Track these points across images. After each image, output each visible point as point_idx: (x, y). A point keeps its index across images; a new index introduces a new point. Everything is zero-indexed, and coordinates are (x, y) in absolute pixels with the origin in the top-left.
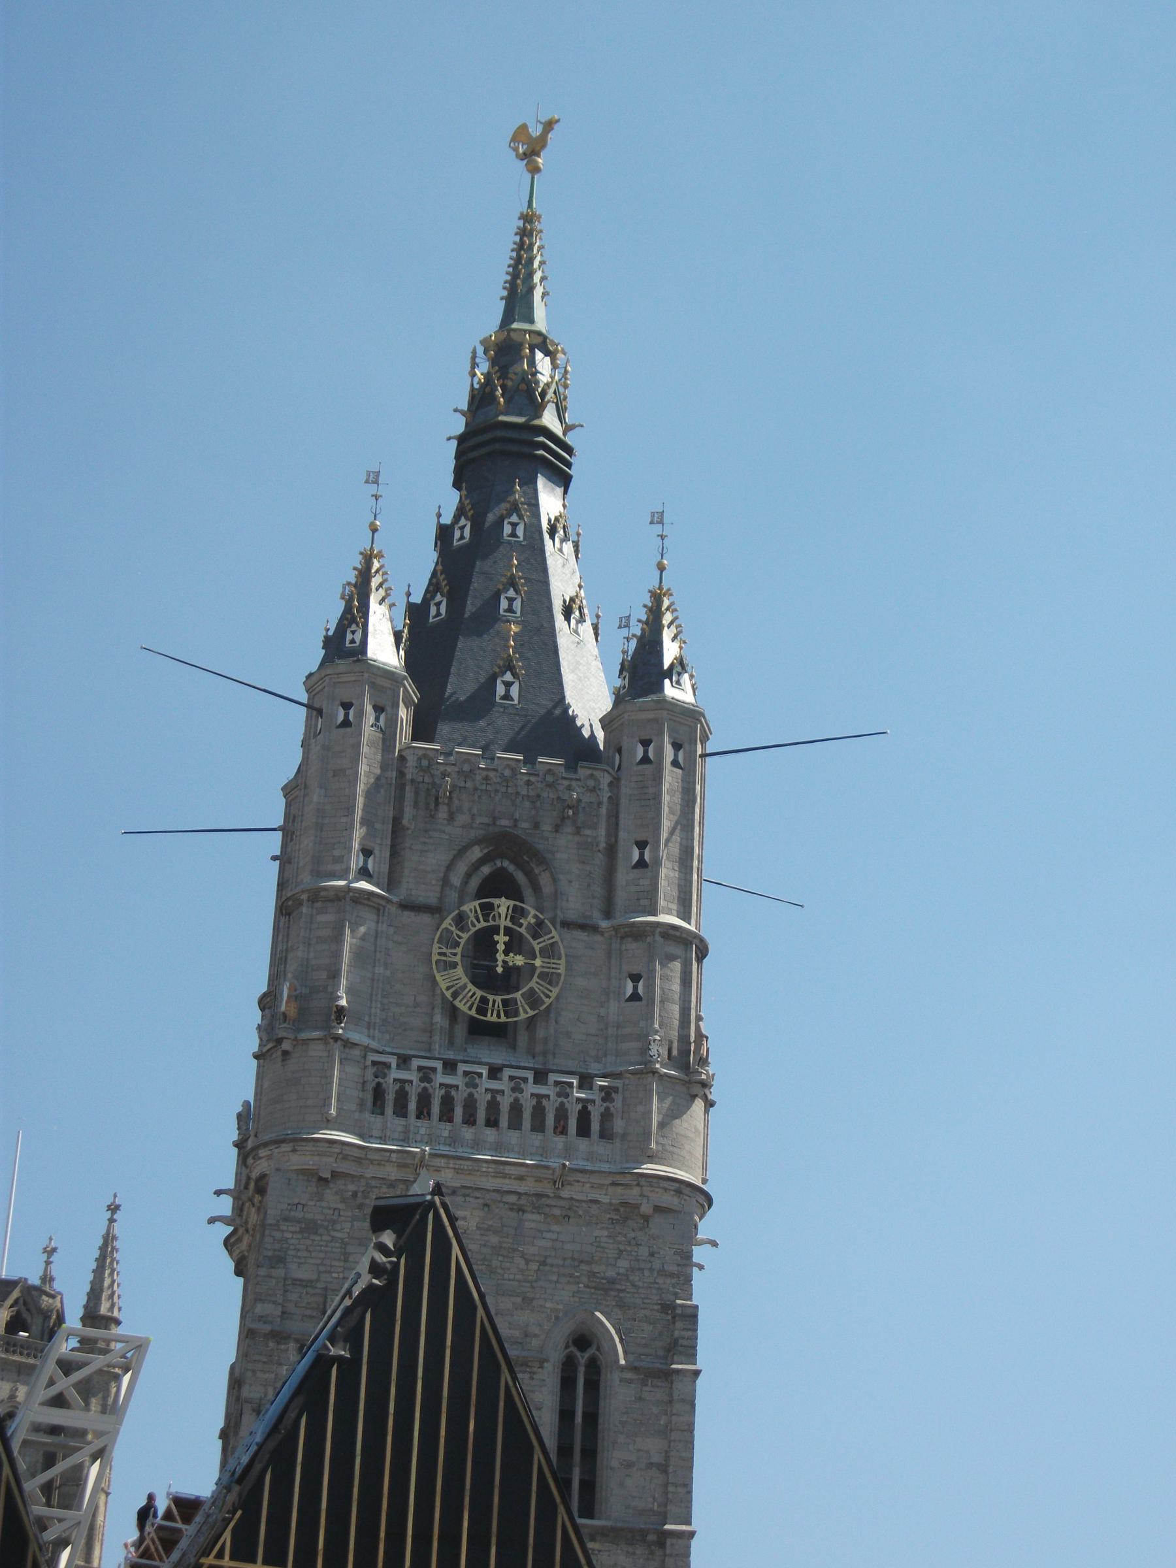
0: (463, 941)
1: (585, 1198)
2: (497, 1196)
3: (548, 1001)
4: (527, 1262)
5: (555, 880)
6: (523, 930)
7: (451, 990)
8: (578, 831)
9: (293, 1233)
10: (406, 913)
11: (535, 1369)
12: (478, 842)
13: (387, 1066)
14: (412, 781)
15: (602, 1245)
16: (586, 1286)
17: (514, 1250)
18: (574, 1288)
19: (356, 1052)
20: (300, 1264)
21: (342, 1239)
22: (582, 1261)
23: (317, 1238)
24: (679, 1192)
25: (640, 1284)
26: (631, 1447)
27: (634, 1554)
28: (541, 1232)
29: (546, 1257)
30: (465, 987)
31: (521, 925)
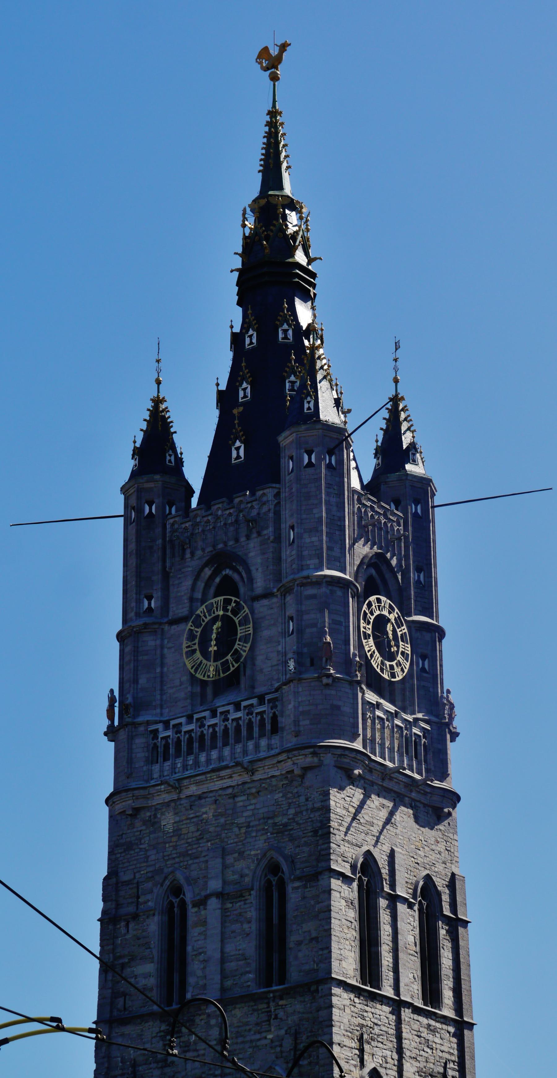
0: (198, 634)
1: (266, 777)
2: (220, 792)
3: (244, 654)
4: (240, 828)
5: (248, 571)
6: (229, 614)
7: (194, 668)
8: (259, 534)
9: (121, 853)
10: (173, 627)
11: (247, 897)
12: (206, 565)
14: (171, 541)
15: (279, 803)
16: (272, 834)
17: (233, 823)
18: (265, 837)
19: (142, 729)
20: (124, 871)
21: (145, 848)
22: (268, 818)
23: (132, 852)
24: (314, 754)
25: (301, 822)
26: (300, 932)
27: (304, 1001)
28: (246, 806)
29: (249, 822)
30: (201, 662)
31: (227, 611)
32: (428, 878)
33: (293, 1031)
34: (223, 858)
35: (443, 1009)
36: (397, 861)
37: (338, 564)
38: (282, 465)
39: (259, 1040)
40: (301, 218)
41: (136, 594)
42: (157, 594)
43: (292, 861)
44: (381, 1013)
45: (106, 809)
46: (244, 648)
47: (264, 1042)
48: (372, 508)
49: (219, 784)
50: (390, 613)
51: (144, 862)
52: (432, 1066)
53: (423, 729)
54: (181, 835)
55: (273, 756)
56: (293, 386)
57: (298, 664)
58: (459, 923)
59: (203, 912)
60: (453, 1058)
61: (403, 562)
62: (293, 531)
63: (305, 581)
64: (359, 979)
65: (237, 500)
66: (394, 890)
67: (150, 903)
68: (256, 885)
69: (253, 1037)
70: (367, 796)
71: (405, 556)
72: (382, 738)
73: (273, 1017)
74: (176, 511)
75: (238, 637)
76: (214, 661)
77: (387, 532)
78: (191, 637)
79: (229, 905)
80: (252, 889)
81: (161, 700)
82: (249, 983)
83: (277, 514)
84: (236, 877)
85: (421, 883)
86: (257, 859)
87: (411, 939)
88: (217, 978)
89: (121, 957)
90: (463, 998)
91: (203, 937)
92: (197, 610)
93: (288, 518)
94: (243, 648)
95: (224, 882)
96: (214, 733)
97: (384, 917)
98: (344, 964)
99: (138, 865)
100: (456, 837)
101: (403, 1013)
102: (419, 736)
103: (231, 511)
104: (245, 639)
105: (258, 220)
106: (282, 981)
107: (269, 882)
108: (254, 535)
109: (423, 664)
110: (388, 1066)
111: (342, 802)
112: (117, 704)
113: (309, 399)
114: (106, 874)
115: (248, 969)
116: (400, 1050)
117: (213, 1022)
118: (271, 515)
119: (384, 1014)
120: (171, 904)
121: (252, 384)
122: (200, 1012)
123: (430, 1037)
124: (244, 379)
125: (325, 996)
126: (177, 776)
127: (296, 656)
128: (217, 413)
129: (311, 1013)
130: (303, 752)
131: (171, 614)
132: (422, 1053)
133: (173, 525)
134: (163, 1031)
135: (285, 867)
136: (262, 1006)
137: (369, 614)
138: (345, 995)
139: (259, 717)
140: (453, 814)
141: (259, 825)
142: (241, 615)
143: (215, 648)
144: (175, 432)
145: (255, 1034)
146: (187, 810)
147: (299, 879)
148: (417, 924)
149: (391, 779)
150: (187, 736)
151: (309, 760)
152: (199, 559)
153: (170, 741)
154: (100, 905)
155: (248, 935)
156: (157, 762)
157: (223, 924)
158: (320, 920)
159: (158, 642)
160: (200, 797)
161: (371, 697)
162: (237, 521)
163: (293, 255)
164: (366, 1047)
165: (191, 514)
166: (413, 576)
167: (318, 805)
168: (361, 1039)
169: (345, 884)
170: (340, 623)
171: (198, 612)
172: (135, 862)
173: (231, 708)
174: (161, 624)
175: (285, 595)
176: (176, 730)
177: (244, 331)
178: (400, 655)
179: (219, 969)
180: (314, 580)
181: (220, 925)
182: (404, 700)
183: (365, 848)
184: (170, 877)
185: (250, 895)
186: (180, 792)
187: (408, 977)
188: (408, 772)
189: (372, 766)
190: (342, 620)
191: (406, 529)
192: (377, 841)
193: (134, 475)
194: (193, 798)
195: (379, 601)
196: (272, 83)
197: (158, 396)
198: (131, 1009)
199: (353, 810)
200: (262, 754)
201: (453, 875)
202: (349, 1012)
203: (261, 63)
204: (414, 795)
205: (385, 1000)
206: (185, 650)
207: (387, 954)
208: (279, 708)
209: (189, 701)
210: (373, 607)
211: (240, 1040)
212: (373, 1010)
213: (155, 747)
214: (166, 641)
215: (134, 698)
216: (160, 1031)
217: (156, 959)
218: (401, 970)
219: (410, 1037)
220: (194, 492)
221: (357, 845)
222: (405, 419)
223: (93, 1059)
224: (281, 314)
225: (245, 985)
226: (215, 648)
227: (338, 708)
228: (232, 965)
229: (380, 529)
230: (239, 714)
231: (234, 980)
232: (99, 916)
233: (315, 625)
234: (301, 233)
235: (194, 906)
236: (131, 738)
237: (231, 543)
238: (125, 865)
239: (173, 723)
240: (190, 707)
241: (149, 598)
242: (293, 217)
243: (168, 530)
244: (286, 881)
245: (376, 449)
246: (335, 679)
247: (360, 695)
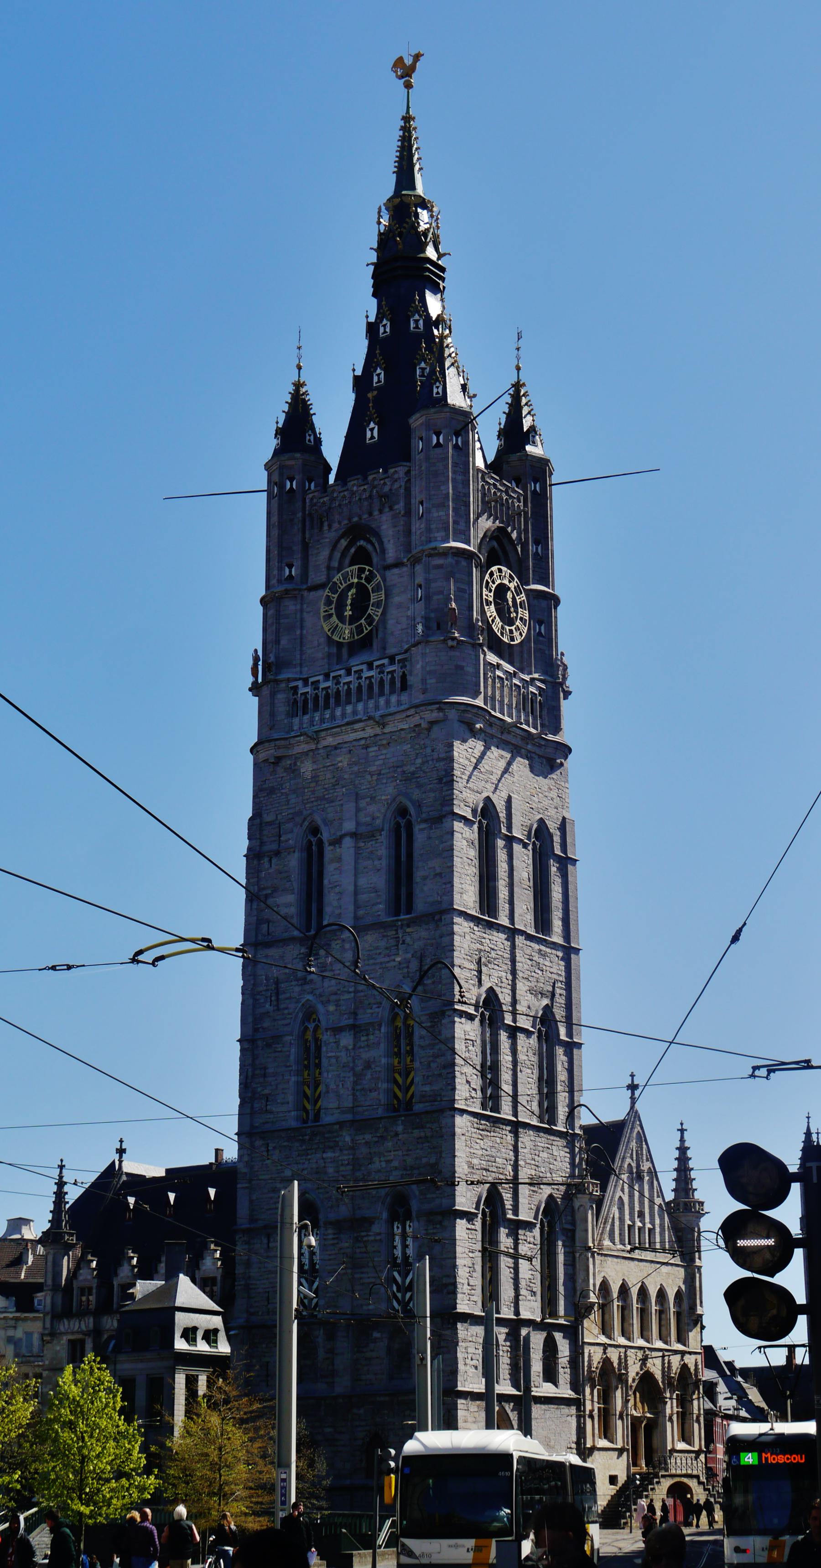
3: (377, 618)
4: (372, 775)
5: (381, 543)
6: (363, 581)
8: (391, 508)
9: (264, 797)
10: (312, 593)
13: (296, 688)
14: (310, 514)
18: (395, 784)
19: (283, 685)
22: (398, 767)
23: (274, 796)
24: (440, 709)
25: (427, 770)
27: (429, 929)
28: (377, 756)
29: (380, 770)
30: (337, 625)
31: (361, 578)
32: (541, 822)
33: (418, 954)
34: (356, 802)
35: (553, 936)
36: (513, 806)
37: (463, 537)
38: (413, 445)
39: (388, 962)
40: (432, 216)
41: (278, 562)
42: (297, 563)
43: (419, 805)
44: (498, 940)
45: (251, 757)
46: (376, 613)
47: (392, 964)
48: (495, 485)
49: (353, 736)
50: (510, 582)
51: (285, 805)
52: (542, 985)
53: (539, 688)
54: (318, 781)
55: (403, 711)
56: (423, 372)
57: (426, 627)
58: (569, 861)
59: (338, 850)
60: (561, 979)
61: (523, 535)
62: (422, 506)
63: (432, 552)
64: (478, 910)
65: (370, 478)
66: (511, 832)
67: (290, 841)
68: (386, 827)
69: (383, 960)
70: (487, 748)
71: (524, 530)
72: (502, 696)
73: (401, 942)
74: (315, 487)
75: (371, 602)
76: (350, 624)
77: (508, 508)
78: (329, 602)
79: (363, 844)
80: (383, 830)
81: (301, 659)
82: (379, 913)
83: (408, 490)
84: (368, 819)
85: (535, 826)
86: (387, 803)
87: (525, 875)
88: (351, 908)
89: (264, 889)
90: (571, 927)
91: (338, 872)
92: (334, 577)
93: (417, 493)
94: (375, 613)
95: (358, 824)
96: (349, 689)
97: (502, 856)
98: (465, 896)
99: (279, 808)
100: (567, 785)
101: (517, 940)
102: (536, 694)
103: (366, 487)
104: (378, 604)
105: (392, 218)
106: (409, 911)
107: (398, 825)
108: (387, 510)
109: (540, 629)
110: (503, 985)
111: (465, 753)
112: (260, 663)
113: (438, 384)
114: (251, 815)
115: (379, 901)
116: (514, 972)
117: (347, 946)
118: (402, 491)
119: (500, 940)
120: (310, 842)
121: (385, 370)
122: (335, 938)
123: (541, 961)
124: (378, 365)
125: (447, 924)
126: (316, 728)
127: (423, 621)
128: (353, 396)
129: (435, 939)
130: (430, 707)
131: (310, 581)
132: (533, 974)
133: (312, 499)
134: (303, 953)
135: (412, 811)
136: (391, 933)
137: (491, 583)
138: (466, 924)
139: (390, 676)
140: (565, 764)
141: (389, 772)
142: (374, 583)
143: (350, 613)
144: (314, 414)
145: (384, 957)
146: (324, 759)
147: (425, 821)
148: (530, 862)
149: (509, 732)
150: (324, 692)
151: (435, 715)
152: (335, 531)
153: (309, 697)
154: (246, 843)
155: (378, 870)
156: (297, 716)
157: (356, 862)
158: (444, 858)
159: (298, 607)
160: (336, 748)
161: (492, 658)
162: (370, 496)
163: (424, 251)
164: (484, 969)
165: (329, 490)
166: (531, 548)
167: (443, 755)
168: (479, 963)
169: (467, 826)
170: (463, 591)
171: (335, 580)
172: (277, 805)
173: (364, 667)
174: (300, 590)
175: (414, 565)
176: (314, 686)
177: (378, 321)
178: (518, 620)
179: (352, 900)
180: (441, 551)
181: (353, 862)
182: (522, 662)
183: (485, 795)
184: (308, 819)
185: (381, 835)
186: (318, 743)
187: (522, 908)
188: (524, 727)
189: (492, 721)
190: (467, 588)
191: (525, 505)
192: (496, 788)
193: (277, 453)
194: (329, 749)
195: (500, 571)
196: (406, 90)
197: (299, 381)
198: (273, 934)
199: (475, 761)
200: (393, 709)
201: (564, 819)
202: (469, 939)
203: (396, 72)
204: (529, 747)
205: (501, 929)
206: (322, 614)
207: (503, 889)
208: (408, 668)
209: (326, 660)
210: (495, 576)
211: (372, 961)
212: (490, 937)
213: (295, 702)
214: (305, 606)
215: (276, 657)
216: (300, 954)
217: (296, 891)
218: (515, 902)
219: (523, 960)
220: (331, 469)
221: (477, 792)
222: (526, 404)
223: (241, 977)
224: (413, 305)
225: (376, 914)
226: (350, 613)
228: (363, 897)
229: (502, 505)
230: (371, 673)
231: (366, 910)
232: (245, 852)
233: (441, 592)
234: (432, 230)
235: (330, 844)
236: (273, 695)
237: (365, 516)
238: (268, 808)
239: (311, 680)
240: (327, 666)
241: (290, 566)
242: (424, 215)
243: (308, 504)
244: (413, 823)
245: (499, 432)
246: (460, 642)
247: (482, 656)
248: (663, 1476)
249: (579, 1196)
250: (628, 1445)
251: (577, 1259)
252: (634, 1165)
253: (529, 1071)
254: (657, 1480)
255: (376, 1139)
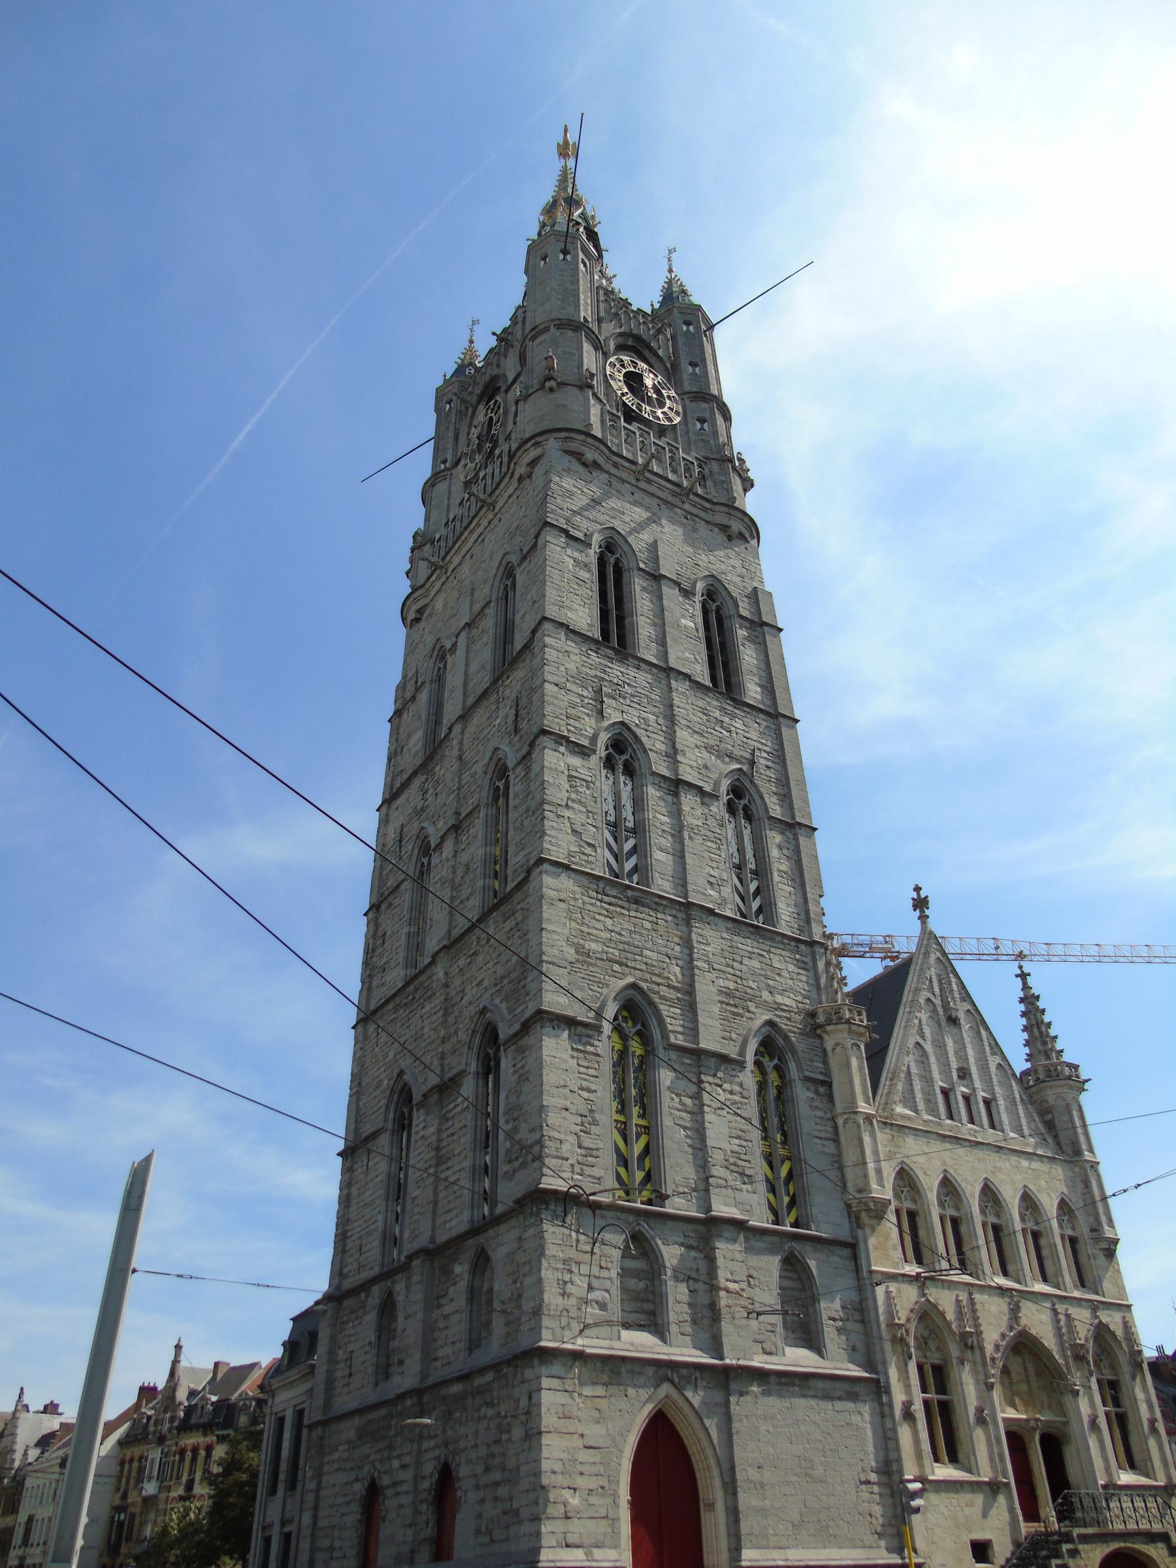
24: (537, 444)
63: (533, 333)
100: (757, 561)
136: (493, 698)
204: (687, 507)
227: (566, 406)
248: (1084, 1539)
249: (828, 1028)
250: (1005, 1476)
251: (841, 1129)
252: (937, 1002)
253: (714, 845)
254: (1070, 1546)
255: (468, 961)
